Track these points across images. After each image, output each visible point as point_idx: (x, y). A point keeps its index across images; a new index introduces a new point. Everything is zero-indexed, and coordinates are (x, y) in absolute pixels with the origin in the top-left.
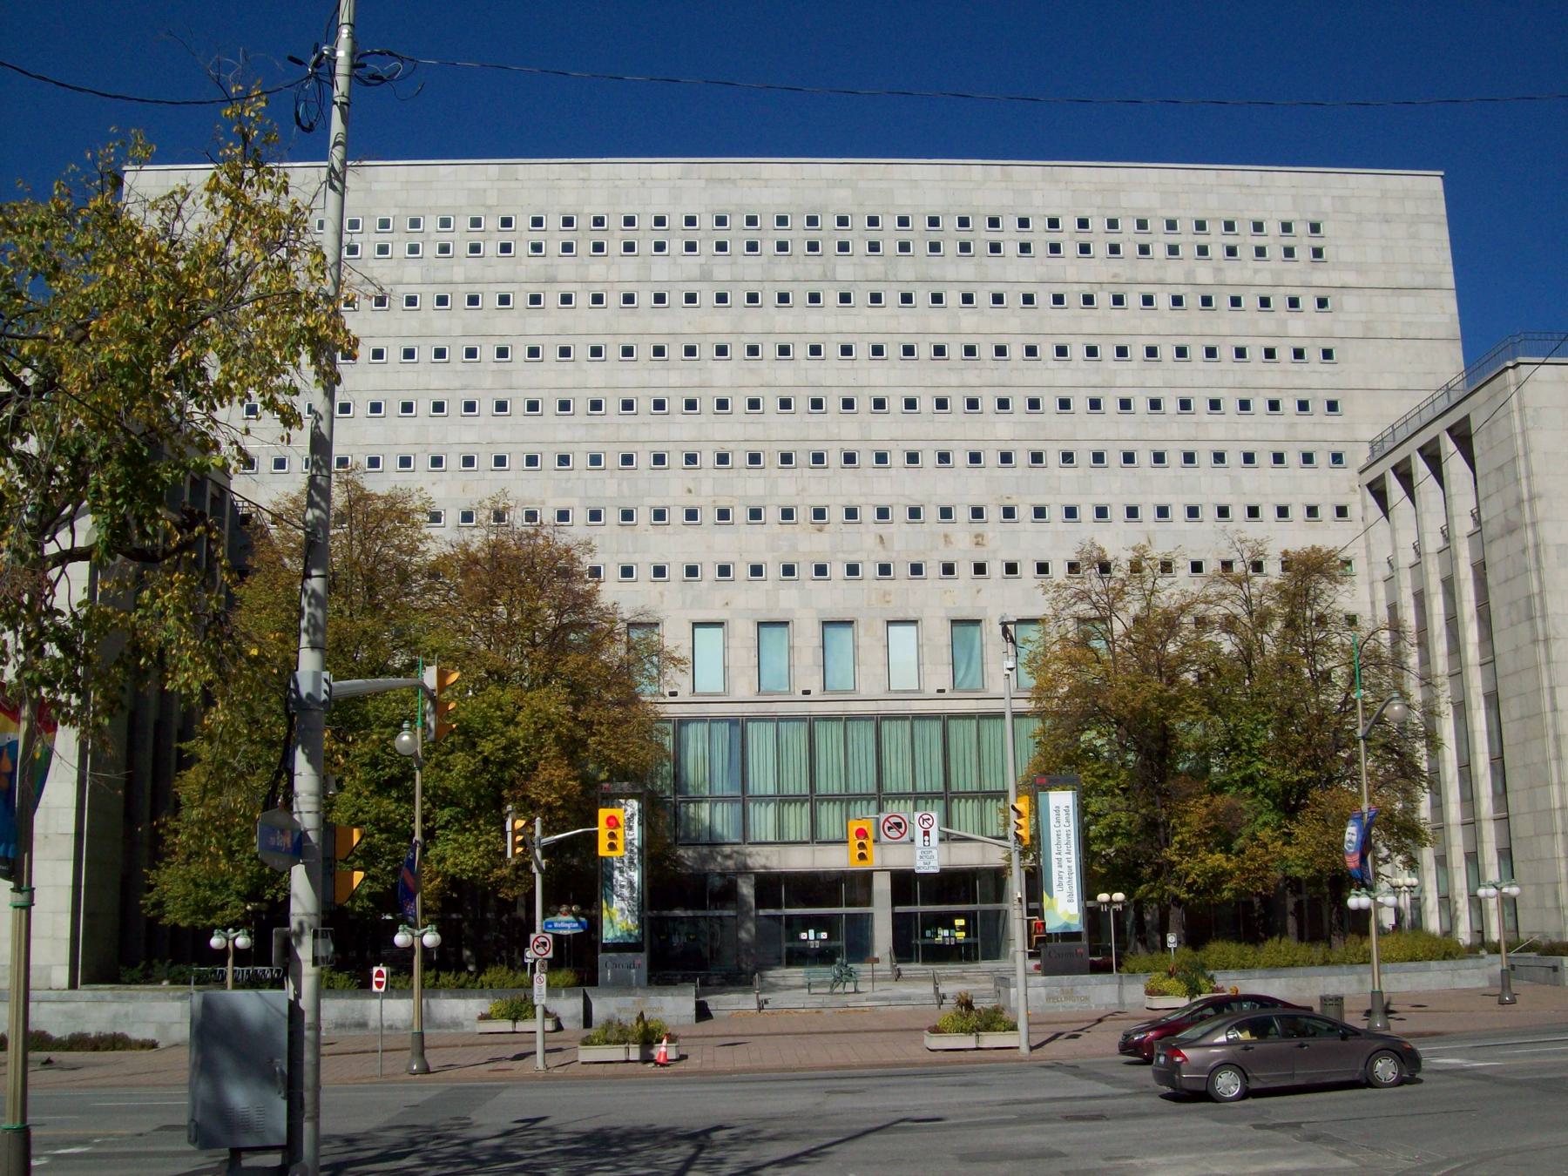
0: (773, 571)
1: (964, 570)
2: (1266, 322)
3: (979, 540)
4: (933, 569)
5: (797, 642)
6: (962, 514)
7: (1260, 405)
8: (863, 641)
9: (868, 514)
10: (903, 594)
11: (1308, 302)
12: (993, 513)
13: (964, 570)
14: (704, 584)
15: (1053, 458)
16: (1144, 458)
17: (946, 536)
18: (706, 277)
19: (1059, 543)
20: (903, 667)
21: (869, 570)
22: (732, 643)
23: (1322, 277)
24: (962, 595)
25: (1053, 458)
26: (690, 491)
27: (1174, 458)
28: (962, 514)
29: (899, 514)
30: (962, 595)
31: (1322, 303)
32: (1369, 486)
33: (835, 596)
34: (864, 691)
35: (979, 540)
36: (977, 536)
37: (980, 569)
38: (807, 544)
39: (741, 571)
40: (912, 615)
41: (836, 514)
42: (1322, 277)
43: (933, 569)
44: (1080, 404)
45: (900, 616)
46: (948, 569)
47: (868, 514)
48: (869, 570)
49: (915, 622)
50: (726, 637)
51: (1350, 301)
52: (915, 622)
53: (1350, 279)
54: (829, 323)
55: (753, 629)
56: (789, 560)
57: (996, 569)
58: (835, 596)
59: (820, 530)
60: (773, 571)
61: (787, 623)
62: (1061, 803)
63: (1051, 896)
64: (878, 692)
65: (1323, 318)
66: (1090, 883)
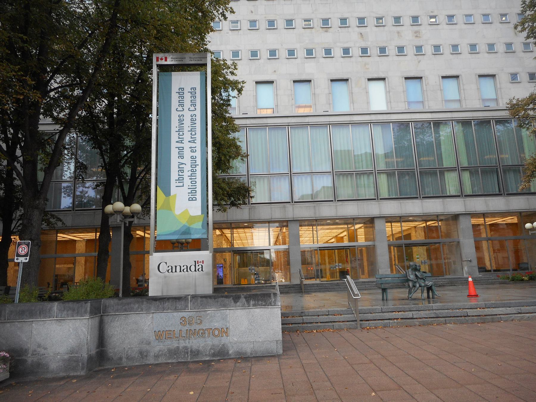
0: (301, 53)
1: (410, 51)
3: (417, 34)
4: (392, 50)
6: (407, 21)
9: (353, 22)
10: (377, 65)
13: (410, 51)
14: (261, 61)
17: (398, 33)
21: (356, 52)
24: (410, 65)
26: (252, 12)
28: (407, 21)
29: (371, 22)
30: (410, 65)
33: (338, 67)
35: (417, 34)
36: (416, 32)
38: (320, 39)
39: (283, 54)
40: (382, 76)
41: (335, 23)
43: (392, 50)
45: (375, 76)
46: (401, 49)
47: (353, 22)
48: (356, 52)
49: (384, 79)
52: (384, 79)
56: (310, 47)
57: (428, 50)
58: (338, 67)
59: (326, 31)
61: (310, 81)
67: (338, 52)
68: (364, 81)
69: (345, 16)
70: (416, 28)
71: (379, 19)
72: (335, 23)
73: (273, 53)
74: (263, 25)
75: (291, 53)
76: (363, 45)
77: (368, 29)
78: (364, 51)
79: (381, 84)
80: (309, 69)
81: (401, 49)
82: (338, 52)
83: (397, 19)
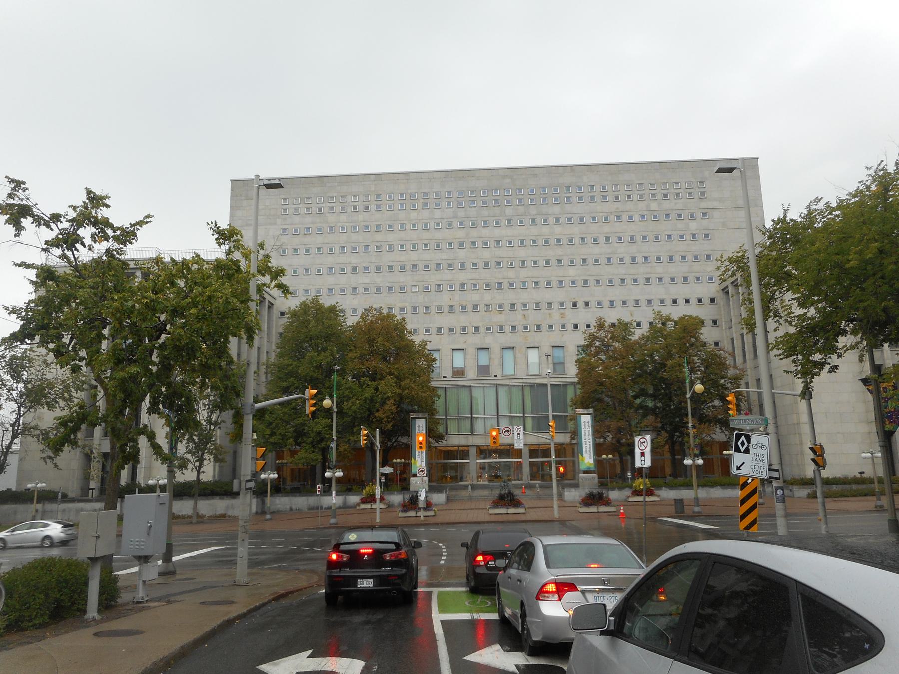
0: (483, 329)
1: (557, 327)
2: (680, 225)
3: (563, 315)
4: (545, 327)
5: (493, 356)
7: (677, 258)
8: (518, 355)
10: (534, 338)
11: (698, 215)
12: (569, 305)
13: (557, 327)
15: (592, 282)
16: (629, 281)
18: (456, 217)
19: (589, 316)
20: (535, 366)
21: (520, 328)
22: (468, 357)
23: (703, 204)
25: (592, 282)
27: (642, 281)
28: (556, 305)
29: (531, 306)
30: (556, 337)
31: (704, 214)
32: (723, 290)
34: (519, 375)
35: (563, 315)
37: (563, 326)
39: (471, 329)
42: (703, 204)
43: (545, 327)
44: (603, 260)
45: (532, 345)
46: (551, 326)
47: (520, 306)
48: (520, 328)
50: (465, 355)
51: (716, 214)
53: (716, 204)
54: (504, 232)
55: (475, 351)
56: (489, 324)
57: (570, 327)
58: (507, 339)
60: (483, 329)
62: (586, 421)
63: (582, 455)
64: (524, 375)
65: (705, 222)
66: (598, 449)
67: (507, 328)
68: (524, 349)
69: (515, 301)
70: (562, 311)
71: (537, 304)
72: (507, 307)
73: (464, 329)
74: (458, 308)
75: (477, 329)
76: (525, 323)
77: (529, 312)
78: (526, 327)
79: (537, 350)
80: (489, 340)
81: (551, 326)
82: (507, 328)
83: (550, 304)
